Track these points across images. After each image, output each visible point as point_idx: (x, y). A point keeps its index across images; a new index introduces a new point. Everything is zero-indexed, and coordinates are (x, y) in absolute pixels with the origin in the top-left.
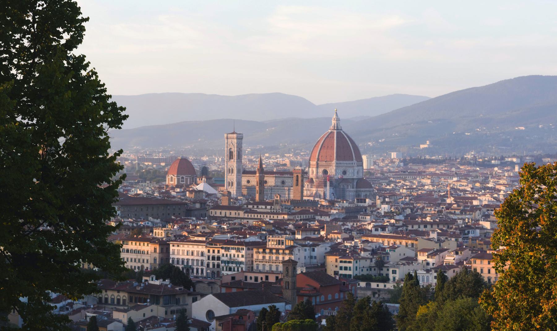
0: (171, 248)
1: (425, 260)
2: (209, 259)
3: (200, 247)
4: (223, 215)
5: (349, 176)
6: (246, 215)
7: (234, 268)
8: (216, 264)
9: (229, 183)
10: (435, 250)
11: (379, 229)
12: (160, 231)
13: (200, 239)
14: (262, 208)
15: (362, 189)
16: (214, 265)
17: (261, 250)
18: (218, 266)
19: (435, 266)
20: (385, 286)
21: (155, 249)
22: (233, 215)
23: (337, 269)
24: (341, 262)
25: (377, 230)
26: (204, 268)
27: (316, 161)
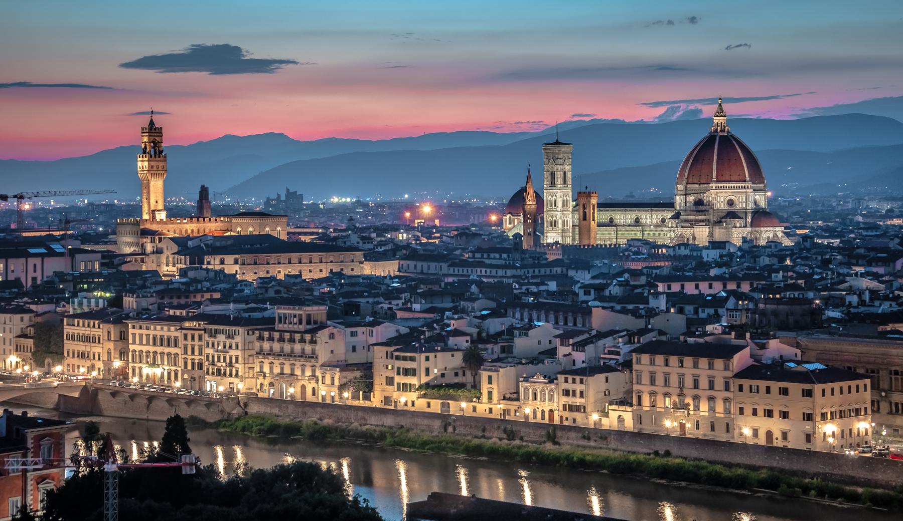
0: (131, 331)
1: (570, 354)
2: (186, 352)
3: (173, 329)
4: (419, 270)
5: (740, 206)
6: (452, 269)
7: (225, 371)
8: (197, 361)
9: (551, 222)
10: (594, 333)
11: (592, 291)
12: (131, 299)
13: (178, 313)
14: (494, 258)
15: (762, 229)
16: (193, 364)
17: (266, 334)
18: (201, 366)
19: (584, 365)
20: (474, 409)
21: (109, 333)
22: (433, 271)
23: (393, 374)
24: (398, 358)
25: (587, 293)
26: (179, 369)
27: (685, 183)
